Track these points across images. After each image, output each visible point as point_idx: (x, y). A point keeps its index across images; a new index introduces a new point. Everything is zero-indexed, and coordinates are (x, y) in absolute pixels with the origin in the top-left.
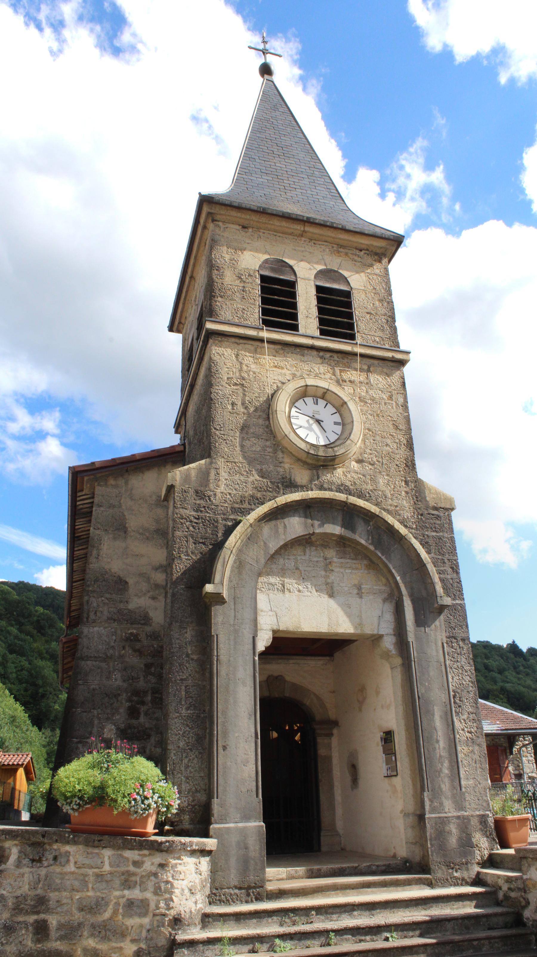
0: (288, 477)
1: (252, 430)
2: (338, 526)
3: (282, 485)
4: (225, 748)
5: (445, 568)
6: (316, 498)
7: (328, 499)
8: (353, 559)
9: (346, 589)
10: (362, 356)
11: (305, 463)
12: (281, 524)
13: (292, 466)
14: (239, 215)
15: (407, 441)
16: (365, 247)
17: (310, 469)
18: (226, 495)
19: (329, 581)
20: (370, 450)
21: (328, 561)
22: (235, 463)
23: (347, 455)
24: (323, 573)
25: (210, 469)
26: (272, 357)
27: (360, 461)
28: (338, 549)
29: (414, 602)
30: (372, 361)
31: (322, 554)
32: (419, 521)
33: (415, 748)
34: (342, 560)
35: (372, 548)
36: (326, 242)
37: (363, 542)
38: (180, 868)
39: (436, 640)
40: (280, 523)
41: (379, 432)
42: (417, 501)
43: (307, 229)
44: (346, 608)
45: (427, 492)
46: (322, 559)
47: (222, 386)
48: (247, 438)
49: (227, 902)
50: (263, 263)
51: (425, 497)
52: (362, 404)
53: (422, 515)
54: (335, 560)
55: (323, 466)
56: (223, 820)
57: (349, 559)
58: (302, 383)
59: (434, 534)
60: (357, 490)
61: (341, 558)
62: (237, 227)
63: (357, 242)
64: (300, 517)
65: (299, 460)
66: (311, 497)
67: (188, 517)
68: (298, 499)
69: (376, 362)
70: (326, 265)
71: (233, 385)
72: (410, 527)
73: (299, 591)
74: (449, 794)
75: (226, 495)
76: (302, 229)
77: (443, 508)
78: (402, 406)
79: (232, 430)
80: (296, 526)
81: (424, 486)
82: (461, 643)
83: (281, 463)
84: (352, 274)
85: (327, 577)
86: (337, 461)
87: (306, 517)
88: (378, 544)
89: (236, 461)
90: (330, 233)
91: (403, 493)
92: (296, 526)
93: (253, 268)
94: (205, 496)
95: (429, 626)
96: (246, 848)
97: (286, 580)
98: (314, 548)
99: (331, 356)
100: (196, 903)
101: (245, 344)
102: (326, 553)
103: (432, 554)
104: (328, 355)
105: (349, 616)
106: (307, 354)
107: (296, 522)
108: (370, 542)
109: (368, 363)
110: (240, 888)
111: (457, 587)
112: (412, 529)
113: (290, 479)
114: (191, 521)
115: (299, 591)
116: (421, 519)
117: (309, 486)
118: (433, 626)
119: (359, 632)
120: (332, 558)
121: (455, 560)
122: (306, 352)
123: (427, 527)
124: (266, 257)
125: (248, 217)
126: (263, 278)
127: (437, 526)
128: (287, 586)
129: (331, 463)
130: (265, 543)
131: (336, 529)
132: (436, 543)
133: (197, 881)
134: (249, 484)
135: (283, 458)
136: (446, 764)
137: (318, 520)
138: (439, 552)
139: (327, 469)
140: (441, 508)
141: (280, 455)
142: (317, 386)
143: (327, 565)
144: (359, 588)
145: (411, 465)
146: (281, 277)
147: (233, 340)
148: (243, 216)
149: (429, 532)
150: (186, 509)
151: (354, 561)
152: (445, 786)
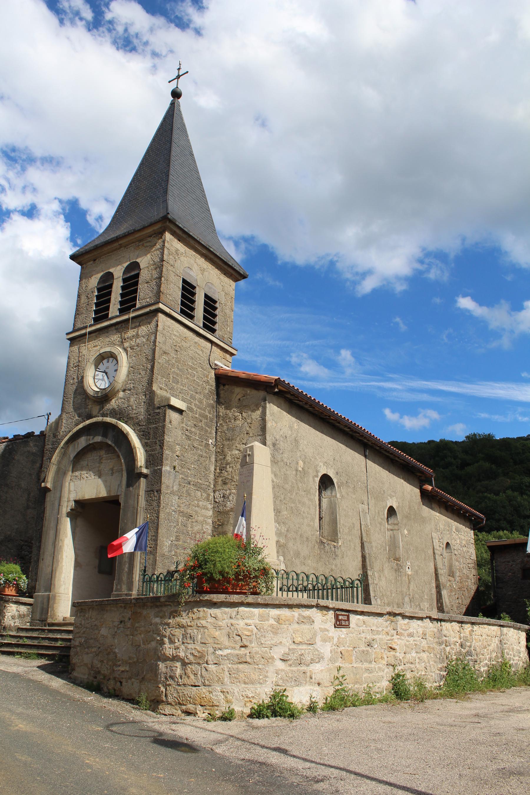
4: (43, 560)
9: (107, 472)
10: (133, 318)
14: (89, 256)
19: (100, 469)
23: (114, 389)
24: (98, 465)
27: (124, 391)
29: (128, 474)
30: (141, 318)
33: (367, 560)
35: (113, 445)
36: (133, 243)
37: (110, 443)
38: (8, 608)
39: (135, 494)
40: (76, 443)
43: (120, 242)
44: (105, 482)
45: (156, 398)
49: (35, 626)
53: (150, 415)
55: (105, 401)
56: (39, 592)
58: (98, 354)
59: (154, 426)
62: (91, 262)
69: (144, 317)
73: (87, 477)
74: (125, 582)
80: (82, 442)
82: (156, 493)
85: (99, 467)
86: (109, 395)
87: (87, 436)
88: (116, 442)
90: (131, 238)
91: (143, 403)
92: (82, 442)
95: (132, 487)
96: (43, 604)
97: (83, 472)
100: (15, 623)
104: (120, 326)
105: (106, 486)
110: (40, 621)
111: (160, 458)
115: (87, 477)
118: (135, 486)
119: (108, 495)
124: (102, 274)
126: (99, 290)
128: (83, 476)
131: (98, 439)
133: (16, 614)
136: (127, 566)
141: (88, 401)
143: (100, 460)
144: (112, 469)
145: (150, 383)
147: (78, 339)
152: (125, 578)
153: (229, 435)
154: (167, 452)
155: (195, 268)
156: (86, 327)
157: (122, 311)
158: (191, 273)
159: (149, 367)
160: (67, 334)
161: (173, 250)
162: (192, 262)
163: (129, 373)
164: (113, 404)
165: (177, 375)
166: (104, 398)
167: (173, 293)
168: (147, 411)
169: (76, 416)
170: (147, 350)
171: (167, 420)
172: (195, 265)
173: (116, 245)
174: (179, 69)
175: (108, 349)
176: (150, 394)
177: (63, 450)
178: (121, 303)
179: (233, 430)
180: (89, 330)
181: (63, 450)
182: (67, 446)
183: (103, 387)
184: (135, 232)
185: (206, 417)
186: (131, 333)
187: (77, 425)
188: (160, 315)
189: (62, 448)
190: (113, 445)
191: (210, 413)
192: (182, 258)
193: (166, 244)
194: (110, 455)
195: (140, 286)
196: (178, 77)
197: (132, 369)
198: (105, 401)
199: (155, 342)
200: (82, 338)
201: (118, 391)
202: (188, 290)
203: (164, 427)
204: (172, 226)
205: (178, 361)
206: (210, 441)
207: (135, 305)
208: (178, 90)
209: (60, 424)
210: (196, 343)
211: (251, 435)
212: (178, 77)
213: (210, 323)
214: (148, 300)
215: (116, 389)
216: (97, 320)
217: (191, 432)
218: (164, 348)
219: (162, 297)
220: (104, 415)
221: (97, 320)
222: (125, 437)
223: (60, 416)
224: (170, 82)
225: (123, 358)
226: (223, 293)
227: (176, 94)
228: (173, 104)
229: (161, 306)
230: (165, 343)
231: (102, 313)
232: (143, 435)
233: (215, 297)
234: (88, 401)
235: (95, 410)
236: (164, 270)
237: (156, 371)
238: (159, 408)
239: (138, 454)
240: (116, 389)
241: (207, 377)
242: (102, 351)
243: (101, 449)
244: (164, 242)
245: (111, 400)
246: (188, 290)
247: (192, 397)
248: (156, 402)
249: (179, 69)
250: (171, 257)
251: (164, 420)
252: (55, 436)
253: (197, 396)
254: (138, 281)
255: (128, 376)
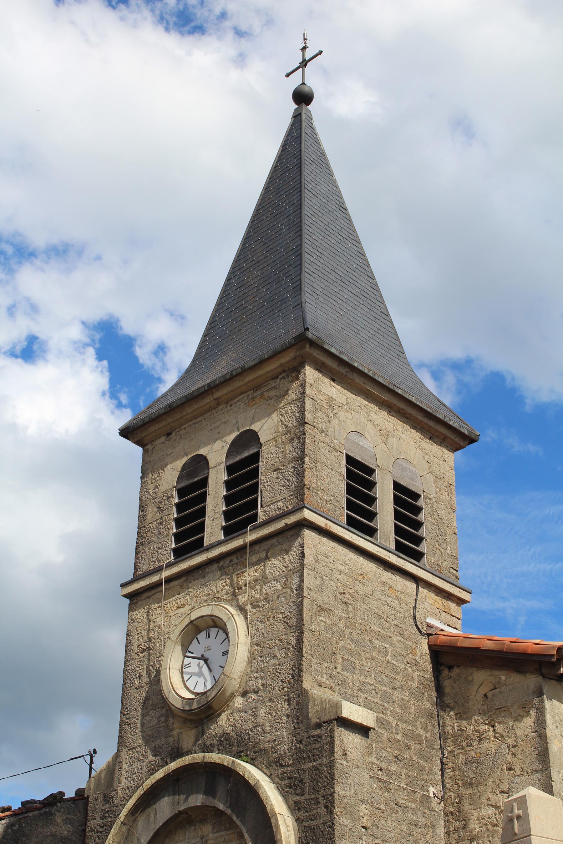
0: (177, 746)
1: (151, 702)
2: (201, 794)
3: (171, 758)
5: (318, 810)
6: (177, 768)
7: (188, 765)
8: (227, 830)
11: (191, 721)
12: (152, 811)
13: (181, 731)
14: (157, 426)
15: (298, 640)
16: (280, 370)
17: (196, 727)
18: (125, 790)
20: (257, 672)
21: (204, 840)
22: (135, 748)
25: (115, 765)
26: (177, 596)
27: (244, 694)
28: (214, 821)
30: (270, 542)
31: (200, 833)
32: (298, 750)
34: (218, 835)
35: (229, 811)
36: (242, 393)
37: (221, 807)
40: (150, 811)
41: (267, 642)
42: (298, 723)
43: (216, 395)
45: (311, 705)
46: (199, 840)
47: (132, 659)
48: (147, 712)
50: (181, 472)
51: (308, 713)
52: (254, 610)
53: (301, 742)
54: (211, 836)
55: (207, 717)
57: (224, 830)
58: (187, 621)
59: (311, 764)
60: (237, 735)
61: (218, 832)
62: (163, 439)
63: (267, 373)
64: (169, 796)
65: (185, 721)
66: (173, 769)
67: (96, 828)
68: (162, 776)
69: (274, 541)
70: (238, 430)
71: (142, 653)
72: (285, 766)
75: (125, 790)
76: (212, 399)
77: (326, 722)
78: (297, 590)
79: (136, 710)
80: (165, 809)
81: (308, 697)
83: (171, 731)
84: (263, 421)
86: (215, 706)
87: (174, 794)
89: (136, 745)
90: (237, 384)
91: (284, 718)
92: (165, 809)
93: (171, 487)
94: (110, 798)
98: (193, 828)
99: (231, 561)
101: (154, 594)
102: (204, 830)
103: (305, 796)
104: (227, 561)
106: (208, 572)
107: (165, 804)
108: (228, 804)
109: (266, 547)
112: (288, 765)
113: (178, 748)
114: (97, 832)
116: (300, 748)
117: (193, 748)
120: (208, 835)
121: (331, 795)
122: (207, 570)
123: (305, 758)
124: (185, 460)
125: (164, 423)
126: (181, 492)
127: (316, 751)
129: (211, 712)
130: (138, 839)
131: (197, 800)
132: (312, 778)
134: (144, 769)
135: (173, 724)
137: (184, 794)
138: (314, 789)
139: (212, 719)
140: (324, 722)
141: (171, 720)
142: (202, 617)
145: (297, 674)
146: (196, 479)
147: (146, 595)
148: (161, 425)
149: (306, 764)
150: (95, 819)
151: (229, 832)
153: (470, 774)
154: (342, 821)
155: (370, 431)
156: (159, 570)
157: (230, 531)
158: (363, 442)
159: (293, 640)
160: (123, 586)
161: (322, 399)
162: (363, 420)
163: (252, 656)
164: (224, 722)
165: (351, 652)
166: (204, 712)
167: (330, 486)
168: (295, 733)
169: (149, 753)
170: (285, 606)
171: (338, 750)
172: (370, 425)
173: (209, 400)
174: (304, 49)
175: (206, 611)
176: (299, 698)
177: (124, 828)
178: (227, 515)
179: (478, 762)
180: (166, 574)
181: (124, 828)
182: (132, 818)
183: (200, 689)
184: (244, 371)
185: (418, 739)
186: (250, 574)
187: (151, 772)
188: (307, 533)
189: (123, 823)
190: (229, 811)
191: (425, 730)
192: (342, 415)
193: (308, 390)
194: (223, 833)
195: (262, 478)
196: (304, 64)
197: (258, 648)
198: (207, 717)
199: (300, 588)
200: (153, 592)
201: (232, 696)
202: (359, 476)
203: (331, 765)
204: (317, 354)
205: (350, 623)
206: (432, 790)
207: (254, 518)
208: (306, 89)
209: (117, 772)
210: (384, 584)
211: (518, 772)
212: (304, 64)
213: (409, 540)
214: (281, 504)
215: (228, 693)
216: (180, 553)
217: (390, 773)
218: (321, 599)
219: (309, 497)
220: (206, 749)
221: (180, 553)
222: (249, 793)
223: (117, 756)
224: (288, 75)
225: (238, 626)
226: (431, 478)
227: (302, 97)
228: (297, 116)
229: (307, 514)
230: (321, 589)
231: (189, 538)
232: (290, 787)
233: (415, 486)
234: (171, 720)
235: (187, 738)
236: (308, 441)
237: (306, 648)
238: (318, 726)
239: (282, 828)
240: (228, 693)
241: (413, 652)
242: (194, 615)
243: (203, 821)
244: (303, 386)
245: (219, 715)
246: (359, 476)
247: (386, 698)
248: (313, 715)
249: (304, 49)
250: (319, 414)
251: (332, 752)
252: (107, 799)
253: (397, 695)
254: (257, 468)
255: (250, 663)
